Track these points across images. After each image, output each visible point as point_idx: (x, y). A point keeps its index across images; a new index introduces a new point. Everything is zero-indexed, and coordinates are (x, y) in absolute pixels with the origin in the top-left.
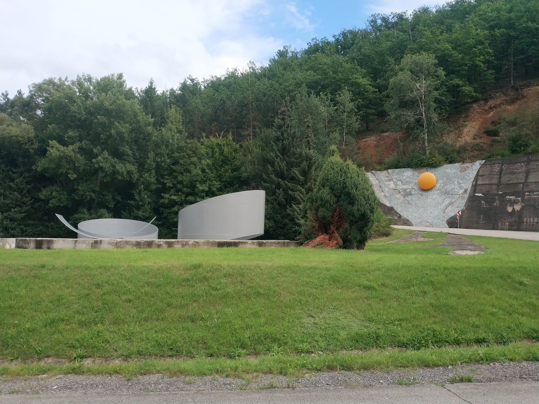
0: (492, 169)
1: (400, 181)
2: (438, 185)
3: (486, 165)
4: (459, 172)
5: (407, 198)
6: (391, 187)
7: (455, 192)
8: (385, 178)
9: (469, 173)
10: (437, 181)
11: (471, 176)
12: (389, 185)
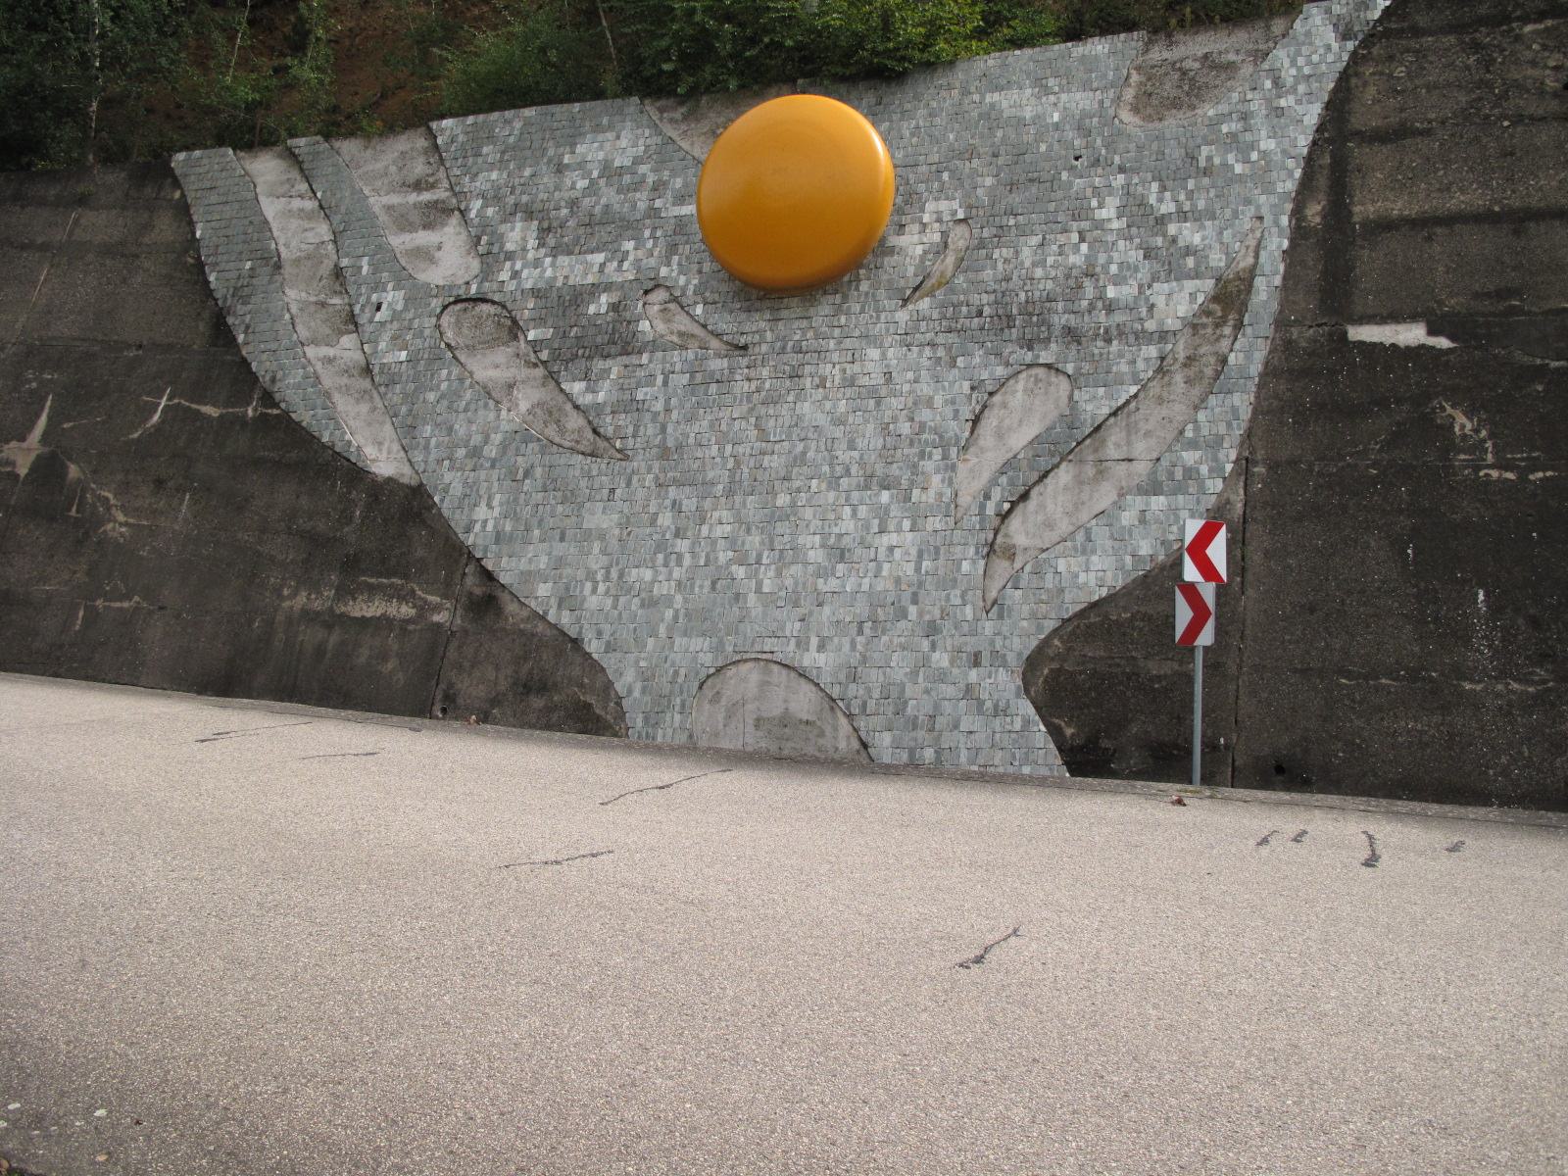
0: (1488, 64)
1: (529, 214)
2: (912, 244)
3: (1417, 32)
4: (1126, 115)
5: (576, 388)
6: (433, 276)
7: (1110, 308)
8: (395, 199)
9: (1245, 117)
10: (909, 200)
11: (1268, 145)
12: (426, 255)
